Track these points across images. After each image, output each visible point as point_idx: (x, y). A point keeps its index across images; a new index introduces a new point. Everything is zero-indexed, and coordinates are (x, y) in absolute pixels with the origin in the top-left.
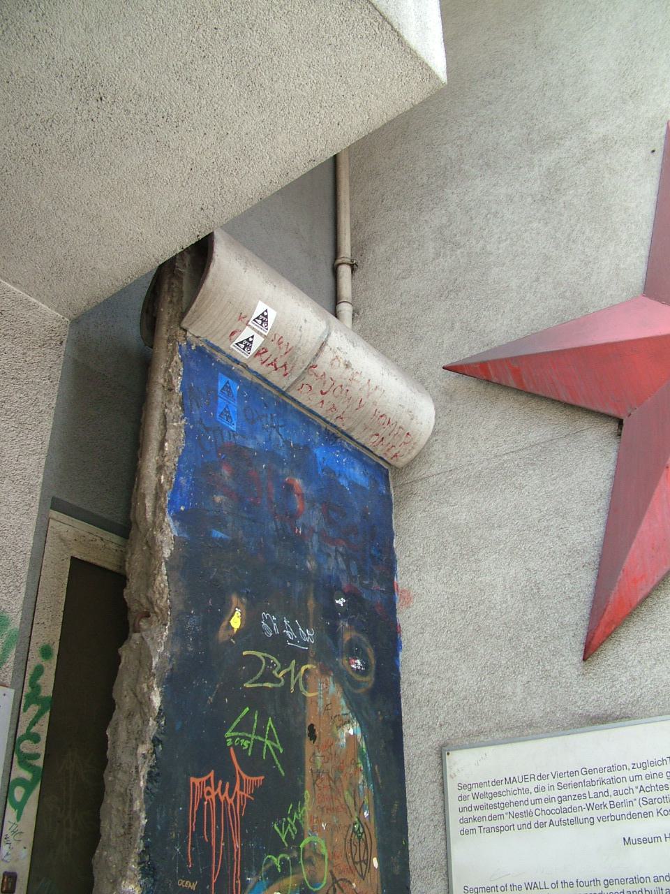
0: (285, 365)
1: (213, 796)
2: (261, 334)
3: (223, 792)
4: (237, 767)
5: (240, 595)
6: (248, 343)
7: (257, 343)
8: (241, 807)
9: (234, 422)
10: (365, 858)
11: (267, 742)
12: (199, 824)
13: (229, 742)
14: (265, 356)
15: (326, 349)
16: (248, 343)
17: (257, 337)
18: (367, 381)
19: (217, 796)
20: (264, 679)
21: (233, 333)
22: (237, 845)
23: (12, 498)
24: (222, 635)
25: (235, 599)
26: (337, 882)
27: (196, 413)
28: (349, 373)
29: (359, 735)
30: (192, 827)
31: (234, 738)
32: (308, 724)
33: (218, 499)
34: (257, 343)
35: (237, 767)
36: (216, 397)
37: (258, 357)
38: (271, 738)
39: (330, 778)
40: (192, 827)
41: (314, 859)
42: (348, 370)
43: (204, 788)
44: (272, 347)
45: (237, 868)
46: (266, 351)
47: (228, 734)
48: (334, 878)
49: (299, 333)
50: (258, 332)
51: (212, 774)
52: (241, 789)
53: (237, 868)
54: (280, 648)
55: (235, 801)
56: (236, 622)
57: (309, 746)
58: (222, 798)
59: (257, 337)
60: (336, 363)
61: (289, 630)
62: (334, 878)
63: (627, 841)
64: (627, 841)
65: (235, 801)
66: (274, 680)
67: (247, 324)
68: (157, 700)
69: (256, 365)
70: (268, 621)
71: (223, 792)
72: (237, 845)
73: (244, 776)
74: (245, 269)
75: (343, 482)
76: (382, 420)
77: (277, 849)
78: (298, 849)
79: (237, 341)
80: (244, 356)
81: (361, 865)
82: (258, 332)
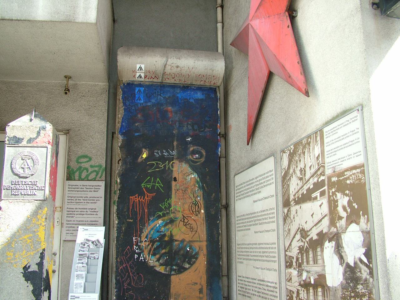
0: (155, 77)
1: (137, 200)
2: (142, 73)
3: (141, 199)
4: (146, 192)
5: (146, 148)
6: (140, 76)
7: (143, 75)
8: (147, 202)
9: (142, 100)
10: (198, 210)
11: (157, 184)
12: (133, 207)
13: (143, 187)
14: (148, 77)
15: (167, 66)
16: (140, 76)
17: (141, 74)
18: (188, 68)
19: (139, 200)
20: (155, 168)
21: (134, 76)
22: (146, 211)
23: (99, 137)
24: (140, 160)
25: (144, 150)
26: (185, 217)
27: (128, 103)
28: (179, 69)
29: (197, 176)
30: (131, 208)
31: (144, 185)
32: (173, 177)
33: (137, 124)
34: (143, 75)
35: (146, 192)
36: (135, 95)
37: (146, 78)
38: (158, 183)
39: (182, 190)
40: (131, 208)
41: (176, 212)
42: (178, 68)
43: (135, 199)
44: (148, 74)
45: (146, 216)
46: (147, 76)
47: (142, 185)
48: (184, 216)
49: (154, 66)
50: (141, 73)
51: (137, 195)
52: (147, 197)
53: (146, 216)
54: (163, 159)
55: (145, 200)
56: (144, 156)
57: (174, 183)
58: (140, 200)
59: (141, 74)
60: (173, 68)
61: (165, 153)
62: (184, 216)
63: (254, 202)
64: (254, 202)
65: (145, 200)
66: (159, 168)
67: (136, 72)
68: (119, 181)
69: (147, 80)
70: (157, 153)
71: (141, 199)
72: (146, 211)
73: (148, 194)
74: (129, 58)
75: (192, 101)
76: (200, 76)
77: (161, 210)
78: (169, 210)
79: (137, 77)
80: (143, 79)
81: (196, 212)
82: (141, 73)
